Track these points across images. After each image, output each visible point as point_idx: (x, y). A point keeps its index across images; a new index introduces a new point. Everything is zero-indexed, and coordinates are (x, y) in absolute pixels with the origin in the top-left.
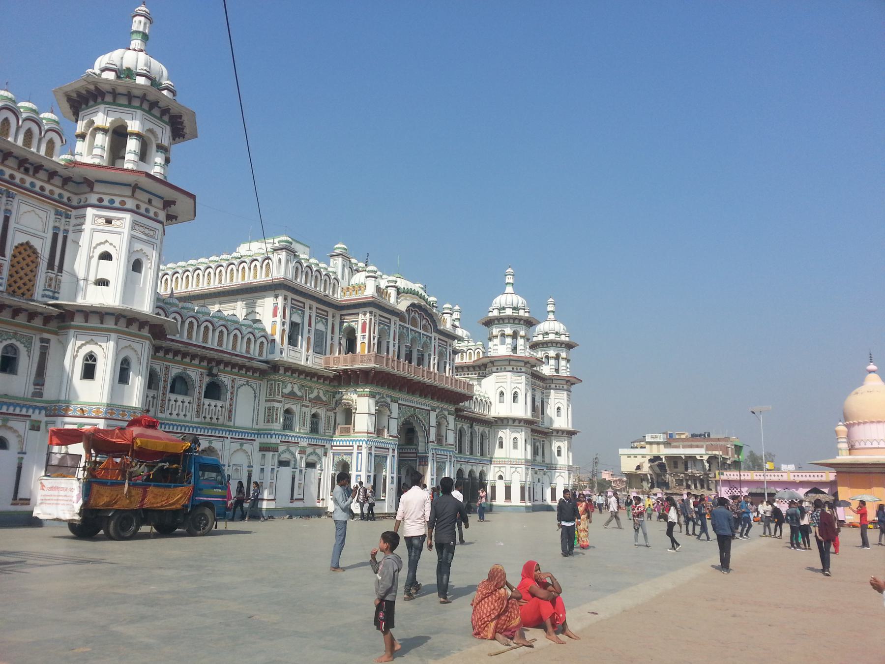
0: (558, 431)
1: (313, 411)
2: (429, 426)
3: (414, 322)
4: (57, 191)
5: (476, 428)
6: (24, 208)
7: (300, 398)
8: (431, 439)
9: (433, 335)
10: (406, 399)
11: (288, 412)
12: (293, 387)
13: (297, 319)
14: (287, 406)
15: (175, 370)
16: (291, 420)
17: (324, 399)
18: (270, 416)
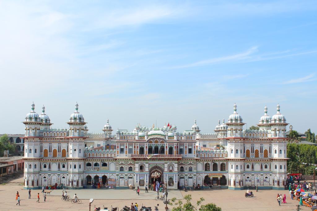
0: (274, 159)
1: (129, 166)
3: (156, 142)
4: (66, 140)
5: (217, 163)
6: (63, 144)
7: (125, 164)
8: (165, 171)
9: (165, 143)
11: (122, 167)
13: (122, 147)
14: (121, 166)
15: (95, 162)
16: (123, 169)
17: (133, 163)
18: (117, 169)
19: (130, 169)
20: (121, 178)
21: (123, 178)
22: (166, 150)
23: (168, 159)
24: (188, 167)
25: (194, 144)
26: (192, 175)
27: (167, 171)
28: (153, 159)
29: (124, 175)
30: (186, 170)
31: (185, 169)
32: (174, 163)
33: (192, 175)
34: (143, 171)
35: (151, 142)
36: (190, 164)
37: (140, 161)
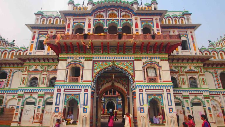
1: (52, 76)
2: (134, 71)
7: (41, 72)
8: (136, 79)
9: (133, 18)
10: (98, 57)
11: (36, 78)
12: (36, 67)
14: (32, 76)
19: (52, 82)
20: (28, 103)
21: (33, 103)
22: (137, 30)
23: (144, 48)
24: (186, 78)
25: (191, 32)
26: (200, 97)
27: (142, 79)
28: (105, 49)
29: (36, 96)
30: (184, 84)
31: (180, 81)
32: (158, 61)
33: (200, 97)
34: (76, 80)
35: (102, 16)
36: (191, 71)
37: (72, 56)
